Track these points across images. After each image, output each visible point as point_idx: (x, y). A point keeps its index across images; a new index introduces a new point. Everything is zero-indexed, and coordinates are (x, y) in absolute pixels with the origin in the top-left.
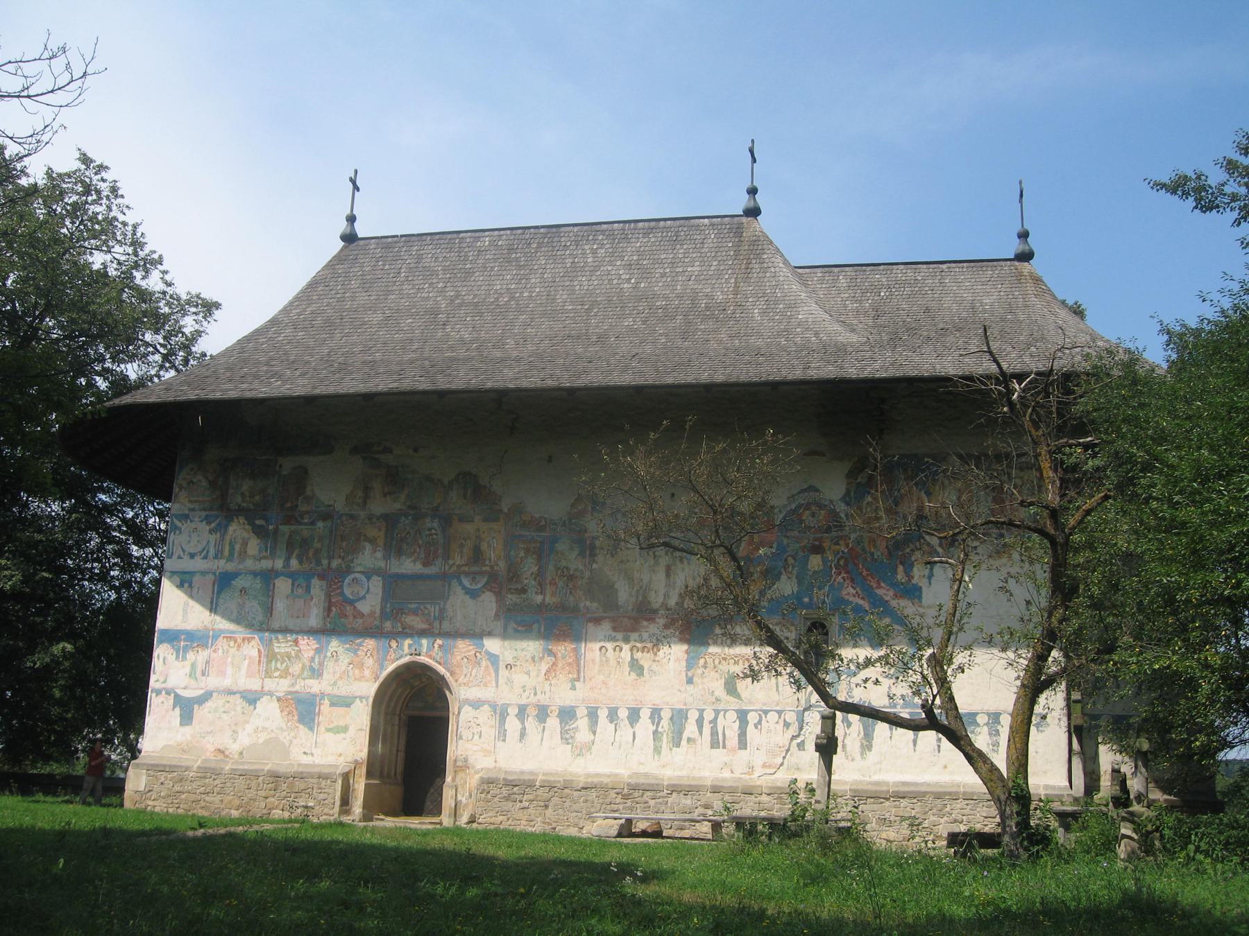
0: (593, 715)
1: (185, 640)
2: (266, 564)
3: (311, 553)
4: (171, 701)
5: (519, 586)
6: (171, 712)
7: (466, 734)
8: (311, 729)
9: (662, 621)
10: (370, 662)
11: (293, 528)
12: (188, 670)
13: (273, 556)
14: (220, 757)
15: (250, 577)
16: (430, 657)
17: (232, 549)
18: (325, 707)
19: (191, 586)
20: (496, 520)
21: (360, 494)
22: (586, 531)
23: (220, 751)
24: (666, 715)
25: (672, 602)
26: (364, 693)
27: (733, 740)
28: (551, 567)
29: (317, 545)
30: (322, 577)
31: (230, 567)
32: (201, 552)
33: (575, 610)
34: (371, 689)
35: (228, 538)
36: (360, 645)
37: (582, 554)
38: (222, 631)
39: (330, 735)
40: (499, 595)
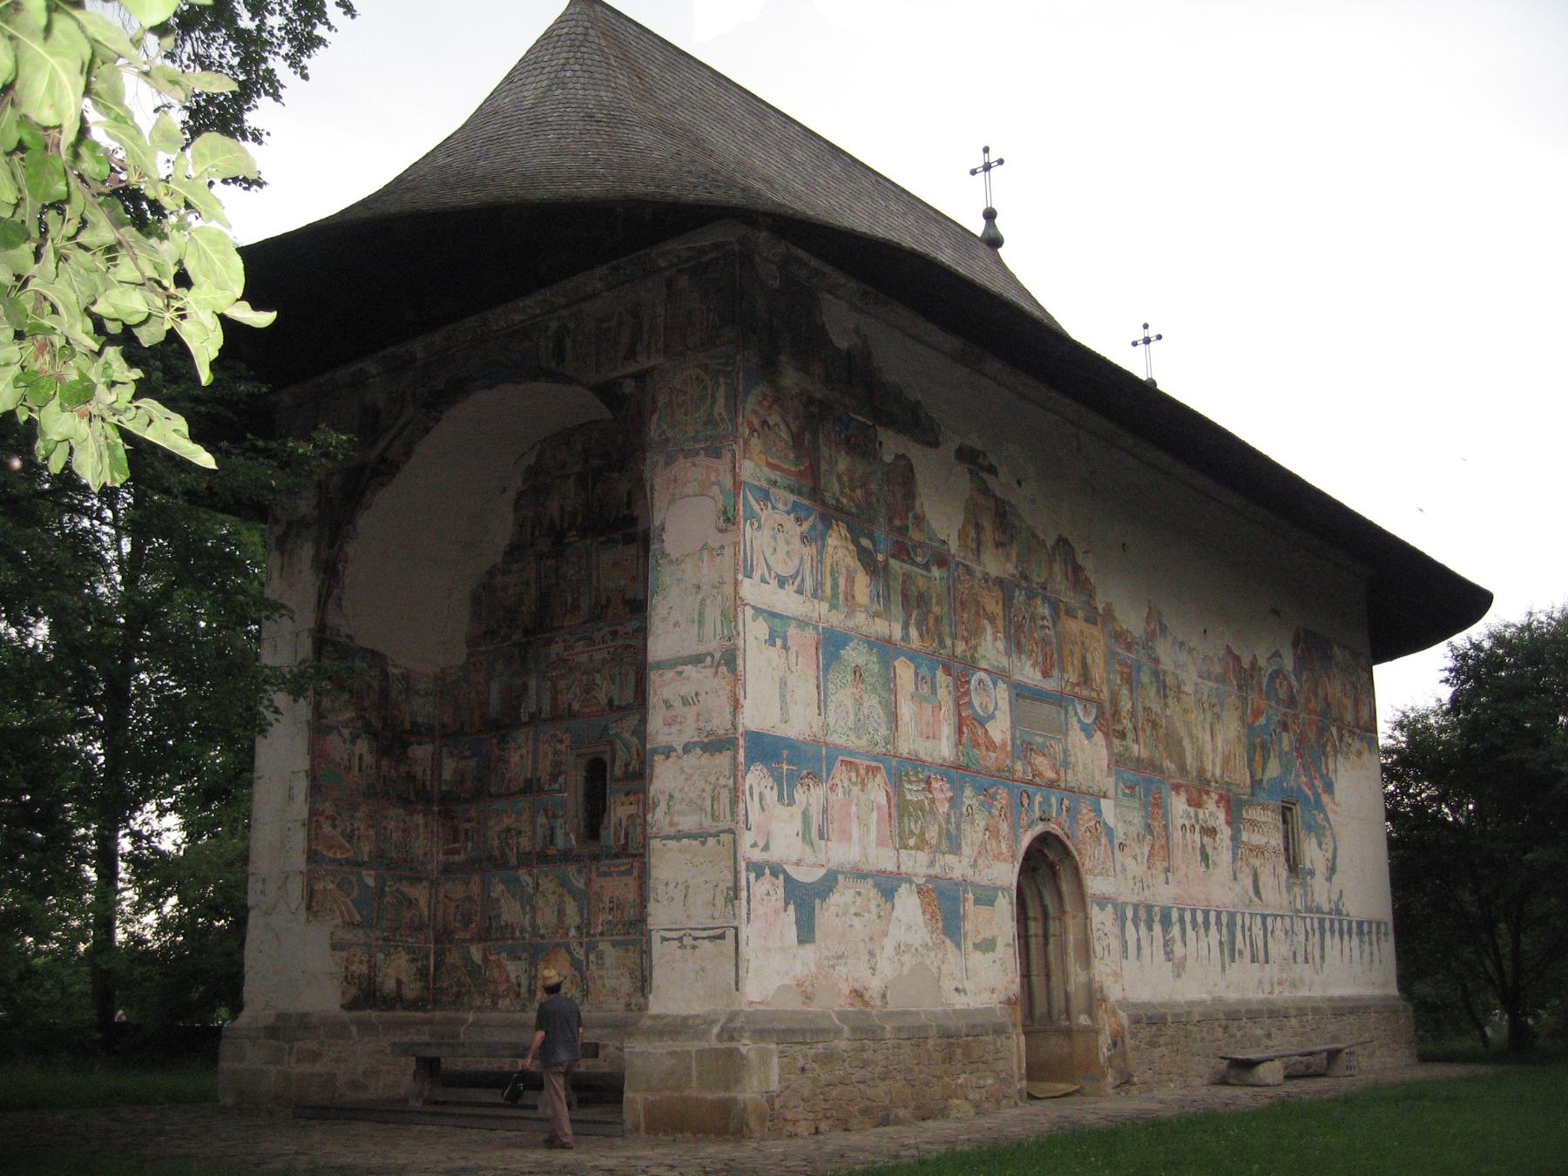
0: (1182, 920)
1: (789, 763)
2: (880, 627)
3: (931, 622)
4: (781, 891)
5: (1119, 727)
6: (782, 915)
7: (1098, 948)
8: (958, 945)
9: (1215, 797)
10: (1004, 827)
11: (907, 567)
12: (798, 825)
13: (885, 614)
14: (859, 1006)
15: (863, 648)
16: (1059, 824)
17: (835, 586)
18: (970, 906)
19: (785, 647)
20: (1095, 623)
21: (973, 534)
22: (1157, 661)
23: (858, 994)
24: (1224, 919)
25: (1218, 772)
26: (1006, 883)
27: (1261, 955)
28: (1140, 706)
29: (936, 609)
30: (947, 670)
31: (836, 619)
32: (794, 577)
33: (1161, 771)
34: (1007, 874)
35: (828, 561)
36: (993, 798)
37: (1158, 692)
38: (836, 747)
39: (978, 955)
40: (1106, 735)
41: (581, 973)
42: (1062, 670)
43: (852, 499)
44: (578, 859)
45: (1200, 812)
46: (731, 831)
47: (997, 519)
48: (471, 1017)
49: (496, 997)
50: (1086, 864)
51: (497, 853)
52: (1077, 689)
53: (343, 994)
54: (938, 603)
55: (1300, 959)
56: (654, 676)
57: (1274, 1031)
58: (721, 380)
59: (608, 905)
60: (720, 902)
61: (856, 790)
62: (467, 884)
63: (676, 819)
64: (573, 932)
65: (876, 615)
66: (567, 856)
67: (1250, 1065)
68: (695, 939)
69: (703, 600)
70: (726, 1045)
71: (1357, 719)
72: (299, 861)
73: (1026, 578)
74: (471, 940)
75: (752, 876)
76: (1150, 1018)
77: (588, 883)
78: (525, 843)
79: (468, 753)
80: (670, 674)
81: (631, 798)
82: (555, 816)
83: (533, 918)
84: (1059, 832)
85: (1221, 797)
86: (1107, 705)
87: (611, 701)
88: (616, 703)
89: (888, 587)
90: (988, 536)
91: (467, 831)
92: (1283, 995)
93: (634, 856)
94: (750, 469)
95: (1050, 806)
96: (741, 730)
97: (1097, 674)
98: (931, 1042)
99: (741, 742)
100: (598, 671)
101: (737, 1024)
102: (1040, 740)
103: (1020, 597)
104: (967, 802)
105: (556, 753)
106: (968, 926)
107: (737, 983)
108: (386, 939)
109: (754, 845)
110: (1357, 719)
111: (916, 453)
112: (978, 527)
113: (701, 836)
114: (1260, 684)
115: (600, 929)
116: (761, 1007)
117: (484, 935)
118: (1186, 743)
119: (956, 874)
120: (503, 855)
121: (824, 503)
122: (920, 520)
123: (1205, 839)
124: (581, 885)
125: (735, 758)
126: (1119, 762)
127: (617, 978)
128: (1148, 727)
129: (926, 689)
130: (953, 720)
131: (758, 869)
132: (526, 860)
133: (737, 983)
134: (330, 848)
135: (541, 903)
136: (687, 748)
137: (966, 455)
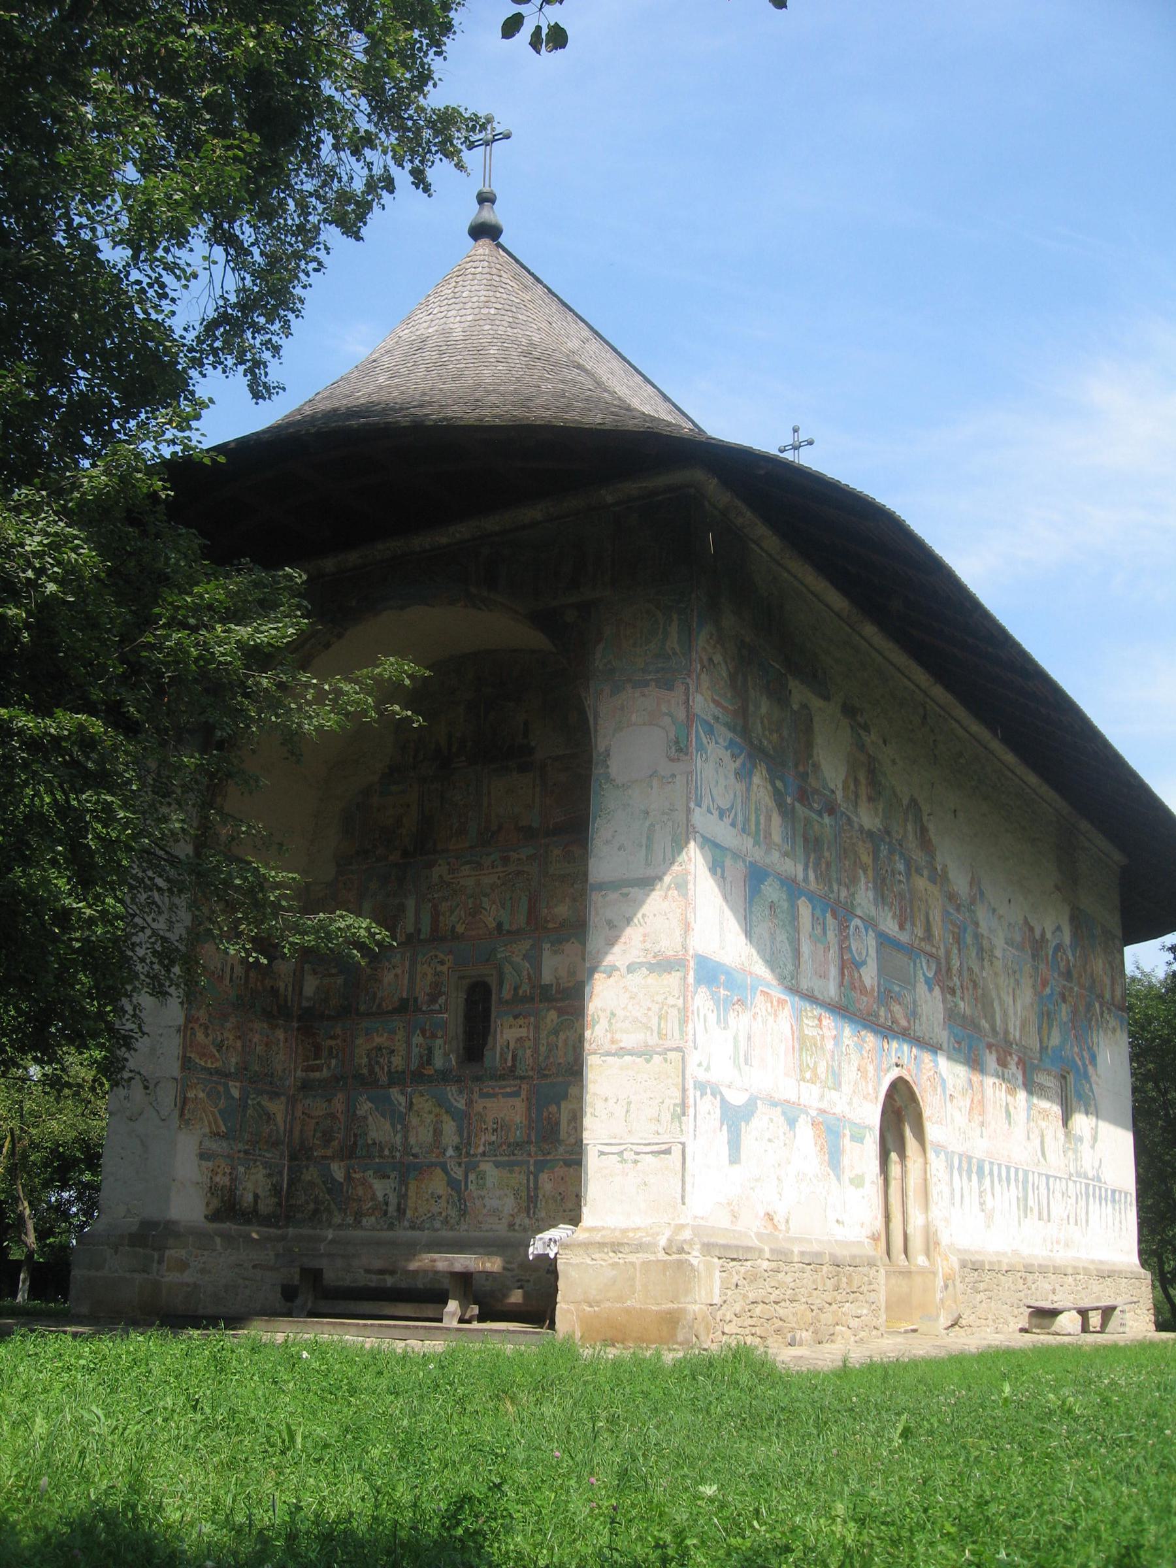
0: (991, 1173)
1: (726, 989)
3: (824, 866)
4: (718, 1111)
5: (951, 985)
7: (935, 1196)
8: (839, 1179)
9: (1016, 1059)
10: (871, 1068)
15: (777, 885)
16: (909, 1071)
18: (846, 1141)
21: (852, 787)
22: (977, 924)
24: (1021, 1174)
31: (757, 854)
32: (730, 810)
34: (871, 1114)
35: (753, 798)
41: (459, 1192)
42: (913, 924)
43: (770, 742)
44: (458, 1081)
45: (1006, 1071)
46: (678, 1049)
47: (868, 775)
48: (330, 1234)
49: (359, 1216)
50: (927, 1112)
51: (365, 1071)
52: (923, 944)
53: (208, 1204)
54: (828, 849)
55: (1072, 1221)
56: (596, 897)
57: (1057, 1286)
58: (675, 616)
59: (491, 1126)
60: (666, 1116)
61: (771, 1019)
62: (329, 1101)
63: (618, 1036)
64: (450, 1152)
65: (786, 854)
66: (445, 1076)
67: (1054, 1313)
68: (638, 1153)
69: (652, 825)
70: (675, 1257)
71: (1113, 998)
72: (175, 1069)
73: (888, 833)
74: (332, 1158)
75: (698, 1094)
76: (973, 1263)
77: (470, 1103)
78: (397, 1061)
79: (334, 971)
80: (613, 896)
81: (521, 1021)
82: (434, 1036)
83: (406, 1137)
84: (908, 1078)
85: (1020, 1058)
86: (943, 961)
87: (500, 926)
88: (506, 927)
89: (793, 829)
90: (863, 791)
91: (331, 1048)
92: (1062, 1256)
93: (522, 1078)
94: (702, 703)
95: (903, 1052)
96: (691, 952)
97: (936, 932)
98: (824, 1268)
99: (692, 964)
100: (486, 895)
101: (687, 1234)
102: (897, 989)
103: (884, 850)
104: (847, 1042)
105: (437, 974)
106: (845, 1161)
107: (683, 1197)
108: (246, 1152)
109: (700, 1065)
110: (1113, 998)
111: (816, 703)
112: (856, 780)
113: (645, 1053)
114: (1047, 955)
115: (481, 1149)
116: (702, 1223)
117: (348, 1153)
118: (996, 1004)
119: (838, 1110)
120: (372, 1071)
121: (751, 743)
122: (816, 767)
123: (1009, 1097)
124: (461, 1104)
125: (685, 978)
126: (952, 1016)
127: (500, 1198)
128: (970, 986)
129: (819, 931)
130: (837, 962)
131: (701, 1087)
132: (397, 1078)
133: (683, 1197)
134: (202, 1055)
135: (415, 1121)
136: (631, 969)
137: (849, 711)
